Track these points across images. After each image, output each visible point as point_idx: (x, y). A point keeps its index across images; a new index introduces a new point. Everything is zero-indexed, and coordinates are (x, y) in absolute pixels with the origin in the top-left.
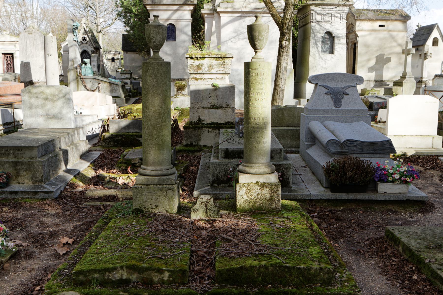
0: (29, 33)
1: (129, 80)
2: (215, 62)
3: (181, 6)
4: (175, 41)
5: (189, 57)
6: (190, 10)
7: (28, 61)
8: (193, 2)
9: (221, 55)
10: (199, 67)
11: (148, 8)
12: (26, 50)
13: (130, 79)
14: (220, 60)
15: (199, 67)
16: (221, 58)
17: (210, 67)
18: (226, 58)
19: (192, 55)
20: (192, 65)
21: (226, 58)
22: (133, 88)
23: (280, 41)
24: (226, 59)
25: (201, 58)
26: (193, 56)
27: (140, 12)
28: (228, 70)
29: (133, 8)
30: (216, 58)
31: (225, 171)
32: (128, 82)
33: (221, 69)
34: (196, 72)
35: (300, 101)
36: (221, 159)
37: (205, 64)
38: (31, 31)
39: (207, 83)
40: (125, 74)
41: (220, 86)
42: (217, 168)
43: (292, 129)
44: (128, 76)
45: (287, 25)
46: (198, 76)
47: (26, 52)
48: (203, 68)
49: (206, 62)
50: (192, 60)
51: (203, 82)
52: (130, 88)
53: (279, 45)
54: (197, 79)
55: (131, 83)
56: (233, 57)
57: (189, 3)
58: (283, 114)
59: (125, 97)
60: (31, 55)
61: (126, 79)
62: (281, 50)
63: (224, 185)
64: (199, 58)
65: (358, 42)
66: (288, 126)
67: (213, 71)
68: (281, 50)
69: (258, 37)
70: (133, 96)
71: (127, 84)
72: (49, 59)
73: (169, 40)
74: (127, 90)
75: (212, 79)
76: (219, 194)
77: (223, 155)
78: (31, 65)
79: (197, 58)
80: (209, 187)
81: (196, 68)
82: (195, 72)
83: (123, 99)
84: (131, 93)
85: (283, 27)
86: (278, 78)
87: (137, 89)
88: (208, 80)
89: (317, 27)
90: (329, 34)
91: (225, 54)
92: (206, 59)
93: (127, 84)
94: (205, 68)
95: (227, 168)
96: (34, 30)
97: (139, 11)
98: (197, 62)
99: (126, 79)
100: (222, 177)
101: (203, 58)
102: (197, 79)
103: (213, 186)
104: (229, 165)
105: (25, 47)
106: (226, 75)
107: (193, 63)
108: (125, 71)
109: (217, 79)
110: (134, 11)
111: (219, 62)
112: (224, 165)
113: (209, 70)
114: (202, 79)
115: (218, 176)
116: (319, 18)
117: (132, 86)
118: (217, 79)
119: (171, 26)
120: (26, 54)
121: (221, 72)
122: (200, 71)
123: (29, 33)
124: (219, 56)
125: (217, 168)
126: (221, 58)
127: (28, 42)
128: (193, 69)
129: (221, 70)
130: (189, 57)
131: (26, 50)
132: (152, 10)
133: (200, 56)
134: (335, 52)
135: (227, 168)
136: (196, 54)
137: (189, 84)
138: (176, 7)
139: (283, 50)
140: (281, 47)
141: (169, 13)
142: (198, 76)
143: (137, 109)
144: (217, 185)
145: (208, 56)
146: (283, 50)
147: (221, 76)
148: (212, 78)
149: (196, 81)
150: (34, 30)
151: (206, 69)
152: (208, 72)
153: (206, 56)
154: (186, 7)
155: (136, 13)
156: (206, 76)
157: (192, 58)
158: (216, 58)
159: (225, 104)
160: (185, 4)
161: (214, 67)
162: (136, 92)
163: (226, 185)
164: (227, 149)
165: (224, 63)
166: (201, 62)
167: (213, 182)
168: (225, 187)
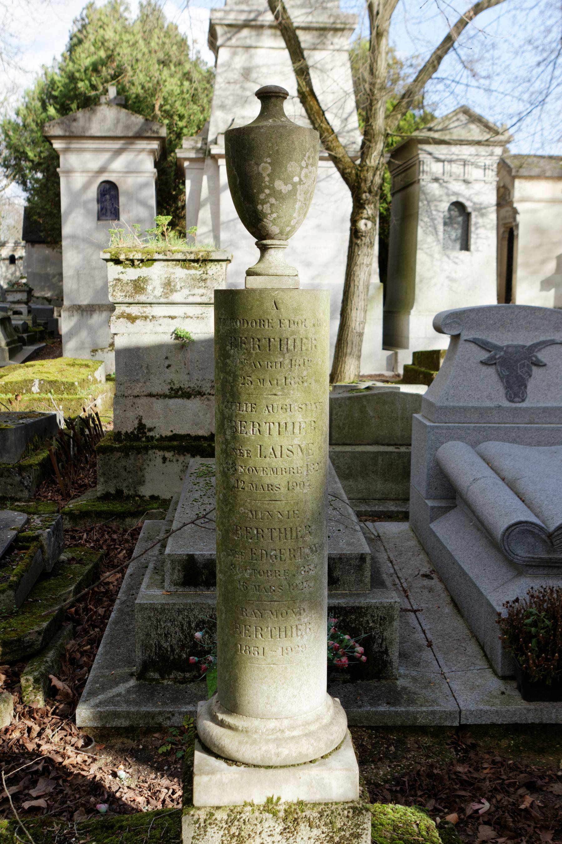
1: (24, 306)
2: (180, 273)
3: (129, 141)
4: (119, 219)
5: (111, 260)
6: (152, 151)
8: (157, 132)
9: (197, 253)
10: (138, 286)
11: (57, 145)
13: (26, 303)
14: (196, 268)
15: (138, 286)
16: (196, 261)
17: (169, 286)
18: (212, 261)
19: (118, 253)
20: (119, 280)
21: (212, 261)
22: (34, 322)
23: (354, 221)
24: (210, 265)
25: (142, 261)
26: (122, 257)
27: (44, 158)
29: (28, 149)
30: (185, 262)
31: (182, 631)
32: (22, 310)
33: (196, 291)
34: (131, 300)
35: (396, 354)
36: (173, 589)
37: (154, 277)
39: (160, 329)
40: (16, 291)
41: (194, 337)
42: (159, 621)
43: (386, 453)
44: (22, 296)
45: (369, 183)
46: (134, 310)
48: (149, 288)
49: (156, 273)
50: (119, 268)
51: (150, 326)
52: (25, 324)
53: (351, 230)
54: (132, 319)
55: (29, 312)
56: (228, 261)
57: (149, 134)
58: (363, 410)
59: (8, 344)
61: (18, 302)
62: (354, 240)
63: (180, 675)
64: (136, 263)
65: (517, 226)
66: (377, 443)
67: (176, 297)
68: (354, 240)
69: (272, 181)
70: (32, 341)
71: (20, 313)
73: (104, 218)
74: (16, 329)
75: (172, 318)
76: (160, 713)
77: (177, 576)
79: (132, 261)
80: (132, 683)
81: (130, 288)
82: (127, 300)
83: (3, 350)
84: (25, 335)
85: (359, 187)
86: (349, 307)
87: (46, 324)
88: (161, 321)
89: (434, 188)
90: (459, 206)
91: (208, 252)
92: (156, 264)
93: (20, 313)
94: (154, 289)
95: (189, 623)
97: (43, 155)
98: (132, 274)
99: (18, 302)
100: (173, 650)
101: (149, 261)
102: (132, 319)
103: (145, 679)
104: (196, 612)
107: (121, 276)
108: (16, 286)
110: (31, 154)
111: (192, 272)
112: (179, 611)
113: (166, 295)
114: (146, 318)
115: (160, 647)
116: (436, 168)
117: (30, 317)
119: (108, 186)
121: (198, 300)
122: (142, 298)
124: (192, 257)
125: (159, 621)
126: (196, 261)
130: (111, 260)
132: (66, 150)
133: (139, 256)
134: (472, 247)
135: (189, 623)
136: (130, 250)
139: (359, 242)
140: (355, 233)
141: (105, 156)
142: (134, 310)
143: (6, 384)
144: (157, 676)
145: (161, 257)
146: (359, 242)
149: (129, 324)
151: (159, 292)
152: (162, 300)
153: (156, 256)
154: (142, 145)
155: (36, 159)
156: (158, 311)
157: (117, 262)
158: (184, 261)
159: (209, 385)
160: (139, 136)
161: (178, 287)
162: (41, 332)
163: (188, 675)
164: (191, 557)
165: (204, 276)
167: (146, 666)
168: (184, 681)
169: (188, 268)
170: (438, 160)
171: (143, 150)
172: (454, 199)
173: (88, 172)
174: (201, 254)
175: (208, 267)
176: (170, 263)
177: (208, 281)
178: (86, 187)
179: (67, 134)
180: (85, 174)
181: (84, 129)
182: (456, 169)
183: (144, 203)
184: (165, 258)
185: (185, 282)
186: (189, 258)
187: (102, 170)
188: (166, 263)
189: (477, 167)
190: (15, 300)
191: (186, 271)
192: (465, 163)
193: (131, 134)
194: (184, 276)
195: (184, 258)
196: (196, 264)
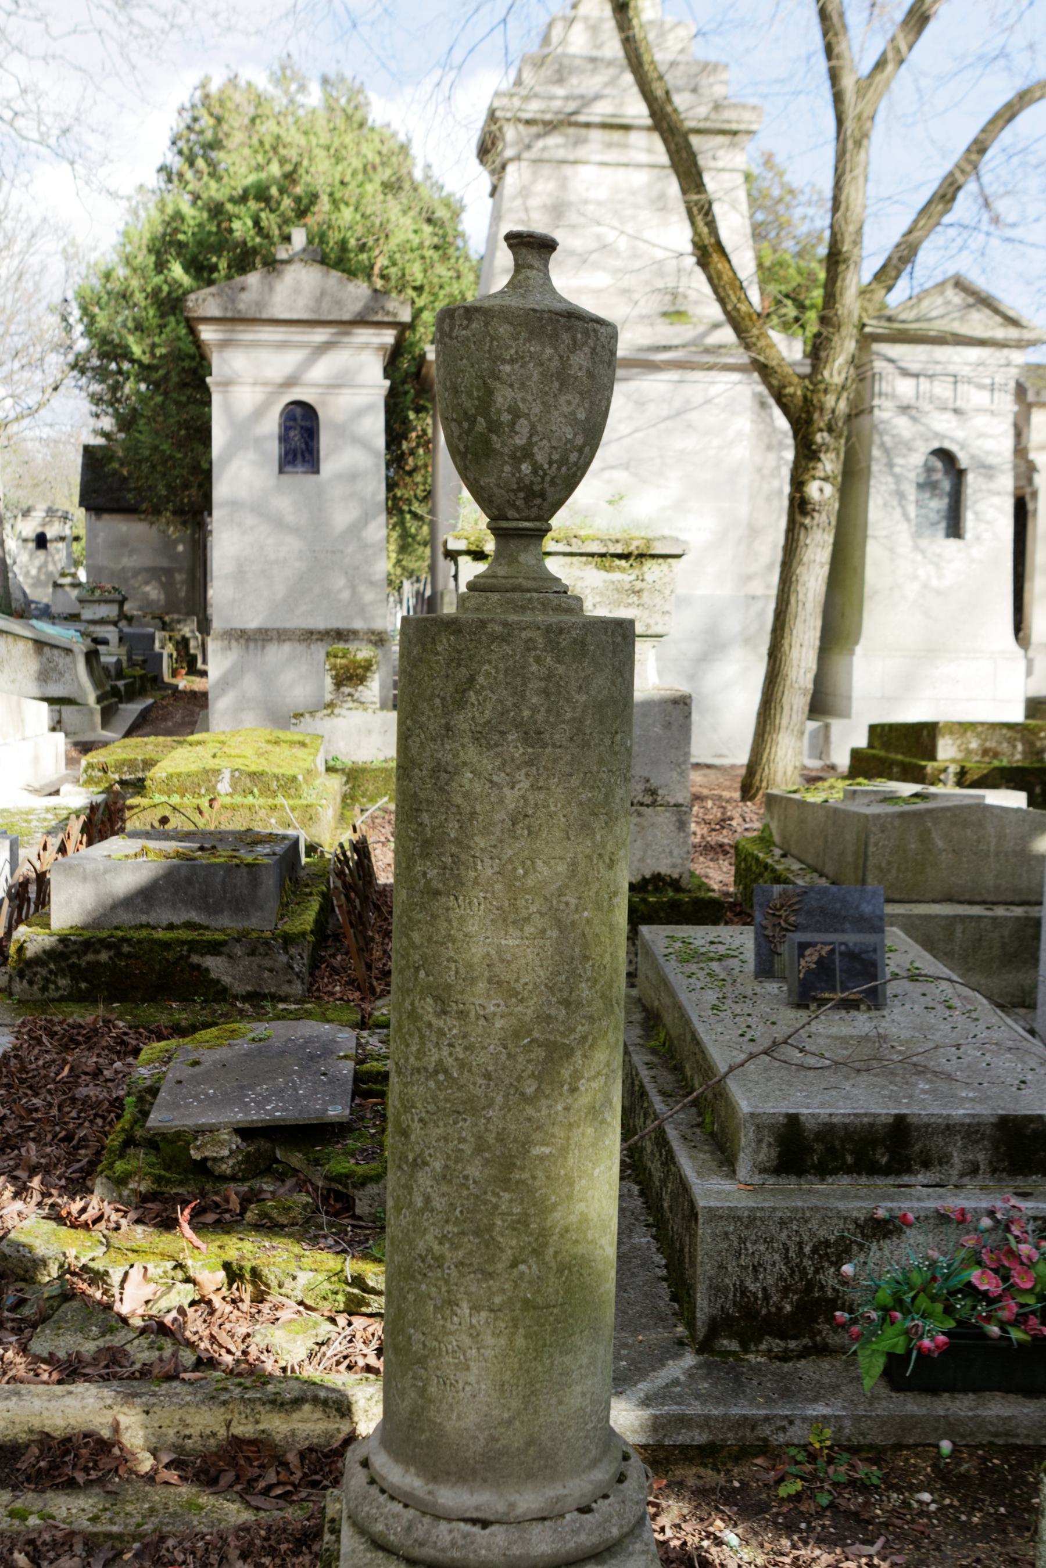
1: (112, 628)
3: (342, 328)
4: (316, 470)
5: (468, 553)
6: (382, 347)
8: (395, 315)
9: (627, 544)
11: (208, 334)
13: (115, 624)
16: (625, 556)
18: (654, 556)
21: (654, 556)
22: (130, 659)
23: (798, 483)
24: (649, 563)
27: (162, 357)
28: (657, 617)
29: (131, 340)
31: (787, 1259)
32: (109, 636)
35: (827, 727)
36: (757, 1179)
40: (99, 601)
42: (743, 1241)
43: (971, 917)
44: (109, 611)
45: (827, 417)
52: (119, 662)
53: (792, 499)
55: (121, 639)
56: (678, 556)
57: (379, 317)
58: (924, 837)
59: (99, 700)
61: (102, 622)
62: (799, 518)
63: (777, 1345)
65: (1034, 494)
66: (949, 899)
68: (799, 518)
70: (131, 694)
71: (105, 642)
73: (289, 469)
74: (106, 669)
76: (767, 1419)
77: (767, 1154)
80: (690, 1359)
83: (91, 711)
84: (121, 684)
85: (809, 422)
86: (786, 642)
87: (145, 661)
89: (902, 425)
90: (945, 456)
91: (649, 540)
93: (105, 642)
95: (800, 1245)
97: (159, 352)
99: (102, 622)
100: (767, 1297)
103: (712, 1352)
104: (814, 1224)
108: (98, 593)
110: (137, 350)
111: (616, 576)
112: (783, 1223)
115: (744, 1291)
116: (905, 387)
117: (123, 650)
119: (299, 411)
124: (619, 549)
125: (743, 1241)
126: (625, 556)
130: (468, 553)
132: (225, 344)
134: (969, 535)
135: (800, 1245)
138: (321, 335)
139: (807, 521)
140: (799, 506)
143: (170, 777)
144: (734, 1346)
146: (807, 521)
154: (364, 335)
155: (146, 359)
158: (603, 555)
159: (640, 787)
160: (361, 321)
162: (142, 677)
163: (792, 1344)
164: (793, 1120)
165: (638, 585)
167: (717, 1327)
168: (785, 1357)
169: (609, 569)
170: (905, 373)
171: (365, 346)
172: (936, 445)
173: (265, 384)
174: (635, 544)
175: (645, 568)
176: (575, 559)
177: (645, 595)
178: (259, 413)
179: (229, 314)
180: (258, 389)
181: (260, 305)
182: (942, 389)
183: (364, 444)
184: (568, 549)
185: (601, 594)
186: (612, 550)
187: (290, 382)
188: (568, 559)
189: (981, 387)
190: (97, 617)
191: (603, 574)
192: (956, 379)
193: (346, 317)
194: (601, 584)
195: (603, 550)
196: (623, 563)
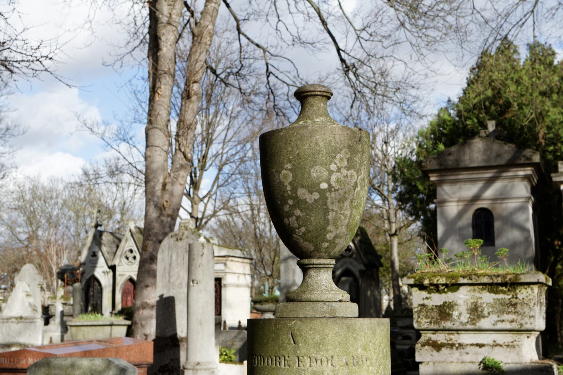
0: (177, 240)
2: (487, 297)
6: (527, 178)
7: (171, 294)
9: (504, 276)
10: (444, 312)
12: (169, 274)
14: (504, 293)
15: (444, 312)
16: (502, 284)
17: (476, 311)
19: (422, 279)
20: (423, 305)
25: (446, 285)
26: (426, 282)
28: (527, 319)
30: (492, 287)
32: (411, 335)
33: (505, 317)
34: (436, 327)
37: (460, 302)
38: (181, 234)
39: (467, 358)
41: (504, 367)
46: (440, 338)
47: (170, 276)
48: (455, 314)
49: (463, 297)
50: (424, 294)
51: (456, 354)
54: (437, 347)
57: (523, 161)
60: (178, 282)
64: (441, 288)
67: (484, 323)
69: (294, 190)
72: (195, 289)
75: (481, 346)
78: (176, 303)
79: (437, 286)
81: (435, 314)
82: (432, 326)
88: (468, 349)
92: (463, 290)
94: (461, 315)
96: (186, 233)
98: (437, 299)
101: (454, 286)
102: (437, 347)
105: (167, 267)
106: (524, 336)
107: (426, 302)
109: (496, 345)
111: (501, 296)
113: (473, 321)
114: (452, 345)
118: (496, 345)
120: (169, 281)
121: (508, 326)
122: (448, 325)
123: (177, 240)
124: (499, 280)
127: (174, 257)
128: (427, 317)
129: (508, 320)
131: (169, 274)
133: (443, 281)
136: (435, 275)
137: (418, 359)
138: (489, 174)
141: (479, 185)
142: (440, 338)
145: (465, 281)
147: (501, 338)
148: (480, 342)
149: (435, 353)
150: (186, 233)
151: (465, 318)
152: (469, 327)
153: (461, 281)
156: (466, 338)
157: (422, 287)
158: (491, 284)
160: (512, 164)
161: (486, 313)
165: (514, 301)
166: (449, 297)
169: (496, 293)
171: (514, 177)
173: (462, 201)
174: (509, 277)
175: (518, 291)
176: (476, 287)
177: (519, 306)
178: (460, 215)
179: (443, 167)
180: (460, 204)
181: (457, 161)
184: (470, 282)
185: (492, 307)
186: (495, 281)
187: (476, 198)
188: (472, 288)
190: (405, 325)
191: (493, 296)
193: (503, 162)
194: (492, 301)
195: (491, 281)
196: (504, 288)
